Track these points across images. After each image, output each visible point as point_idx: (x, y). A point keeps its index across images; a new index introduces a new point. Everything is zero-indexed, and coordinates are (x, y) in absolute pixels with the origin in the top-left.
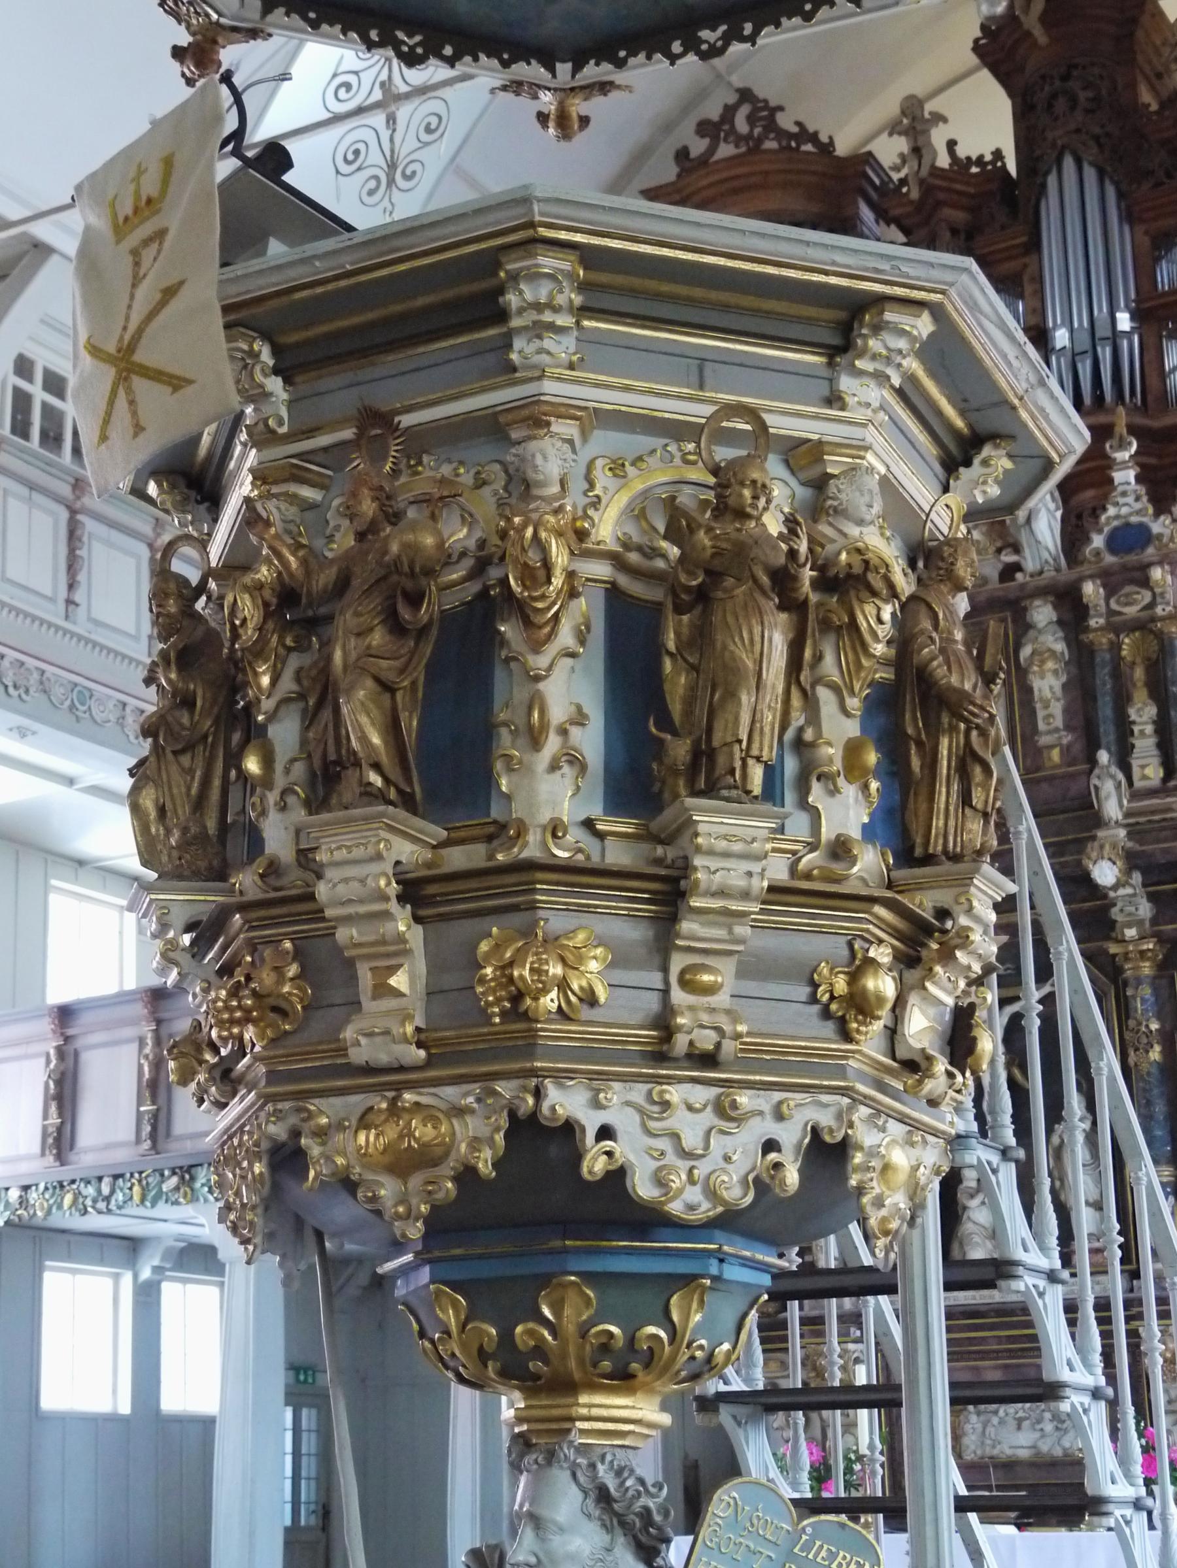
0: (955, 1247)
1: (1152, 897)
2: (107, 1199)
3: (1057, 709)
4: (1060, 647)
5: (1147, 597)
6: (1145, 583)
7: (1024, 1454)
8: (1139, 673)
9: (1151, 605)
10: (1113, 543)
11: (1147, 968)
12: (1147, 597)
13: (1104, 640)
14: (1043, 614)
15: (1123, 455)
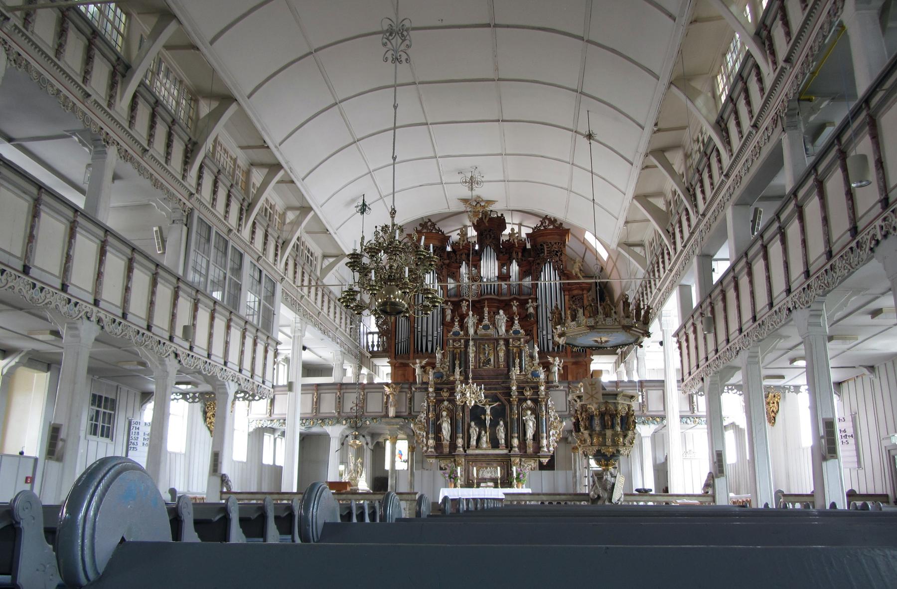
0: (479, 444)
1: (518, 392)
2: (304, 424)
3: (503, 358)
4: (504, 348)
5: (519, 343)
6: (520, 340)
7: (489, 477)
8: (517, 355)
9: (520, 344)
10: (513, 333)
11: (516, 403)
12: (519, 343)
13: (511, 348)
14: (502, 342)
15: (516, 318)
